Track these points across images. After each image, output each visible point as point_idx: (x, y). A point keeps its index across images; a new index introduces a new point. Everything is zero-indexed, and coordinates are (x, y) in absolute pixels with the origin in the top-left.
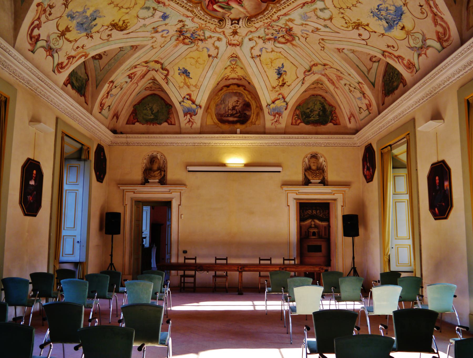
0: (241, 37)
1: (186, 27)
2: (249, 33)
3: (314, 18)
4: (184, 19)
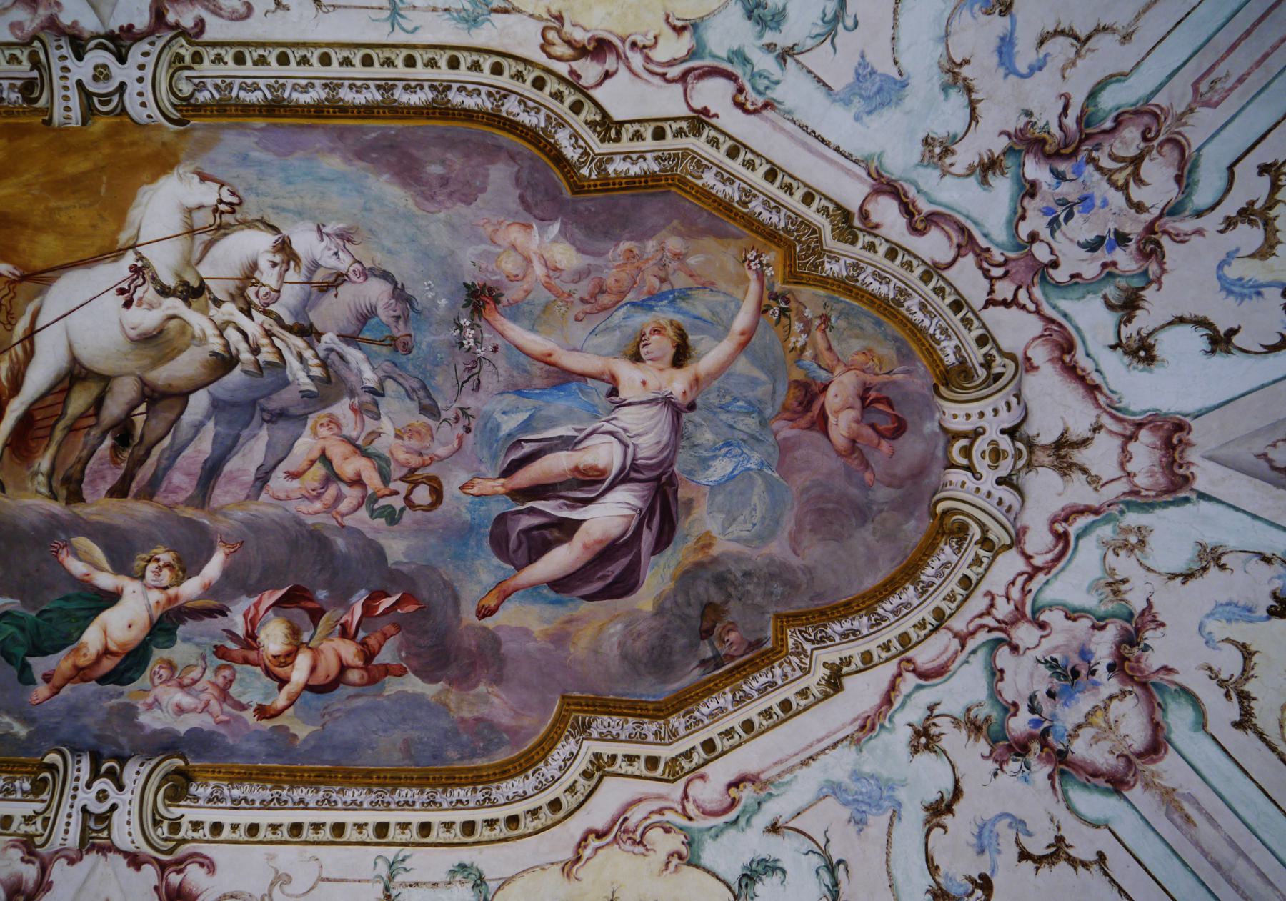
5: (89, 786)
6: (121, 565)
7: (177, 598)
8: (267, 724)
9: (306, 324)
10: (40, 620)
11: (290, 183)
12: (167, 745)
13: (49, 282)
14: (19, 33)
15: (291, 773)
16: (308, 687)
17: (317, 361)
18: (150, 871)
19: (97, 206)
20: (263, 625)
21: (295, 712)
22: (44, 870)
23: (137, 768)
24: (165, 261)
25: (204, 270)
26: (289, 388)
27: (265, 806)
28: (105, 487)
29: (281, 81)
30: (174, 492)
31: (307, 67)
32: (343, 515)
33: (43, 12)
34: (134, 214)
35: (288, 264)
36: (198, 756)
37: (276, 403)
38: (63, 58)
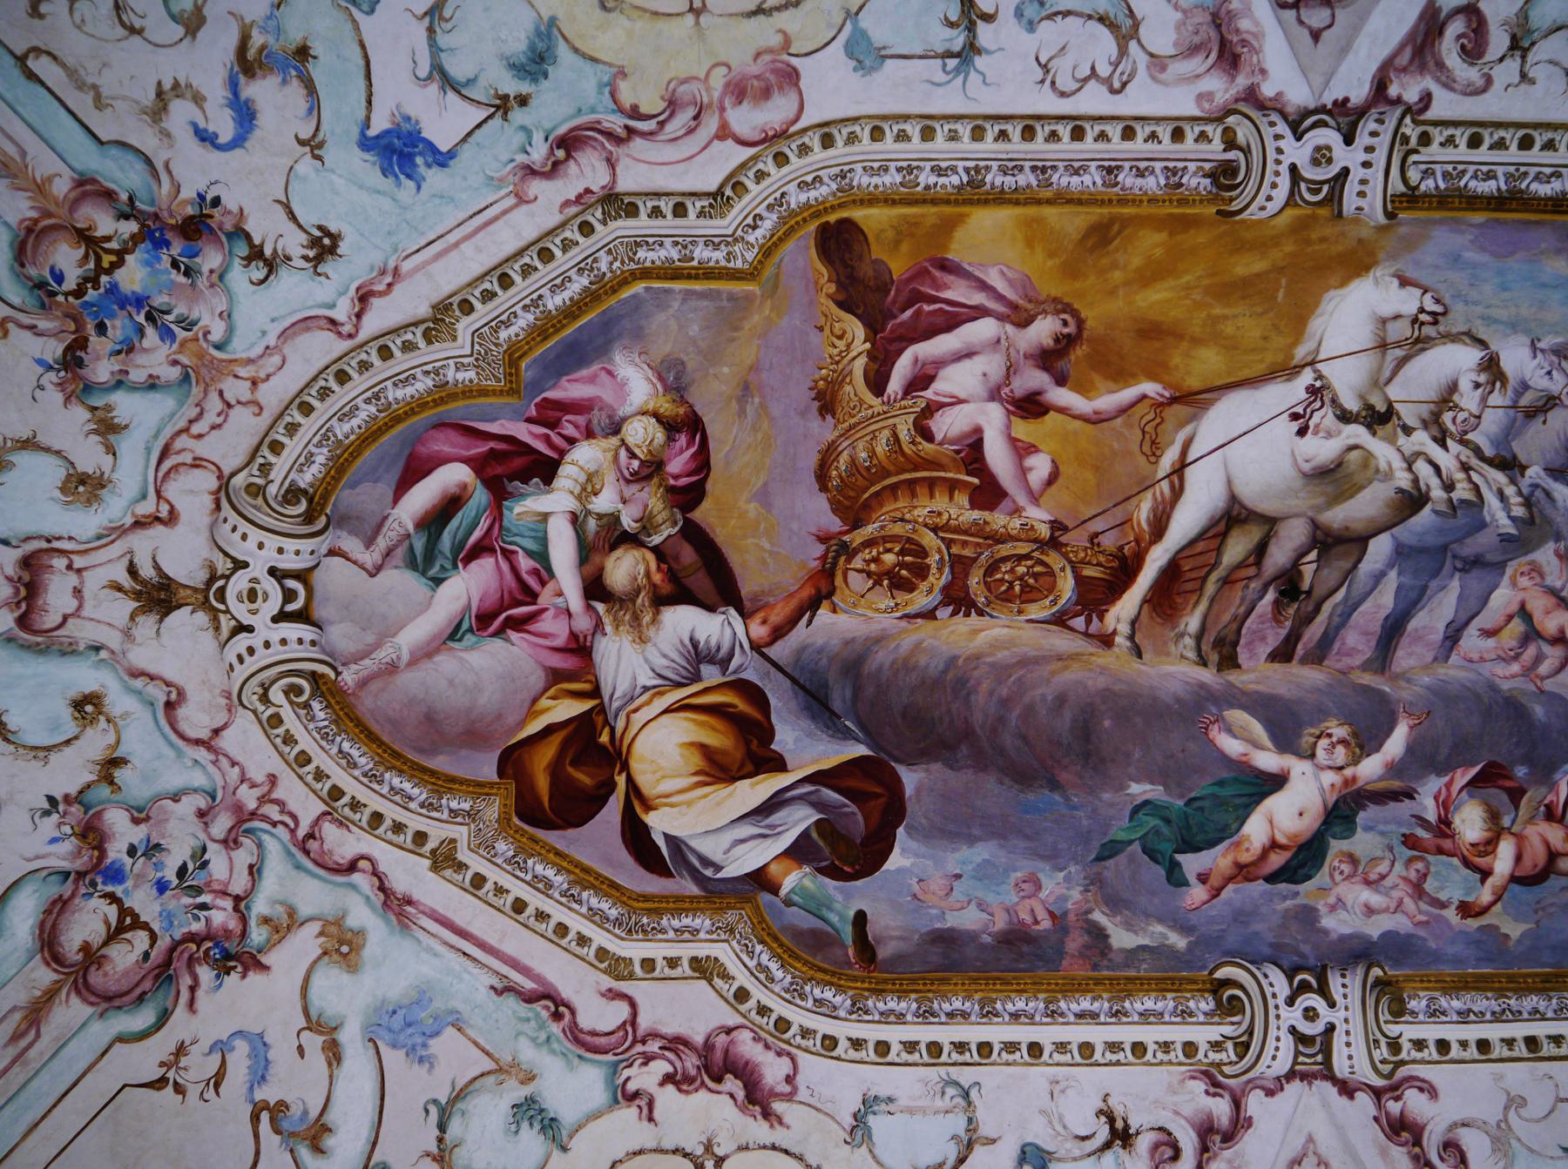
0: (113, 639)
1: (239, 277)
2: (159, 694)
3: (414, 1087)
4: (347, 272)
5: (1291, 1002)
6: (1285, 741)
7: (1354, 779)
8: (1473, 924)
9: (1508, 456)
10: (1189, 810)
11: (1505, 289)
12: (1358, 953)
13: (1205, 406)
14: (1207, 106)
15: (1511, 978)
16: (1514, 879)
17: (1519, 499)
18: (1363, 1098)
19: (1271, 314)
20: (1457, 808)
21: (1504, 908)
22: (1237, 1104)
23: (1340, 980)
24: (1347, 380)
25: (1393, 392)
26: (1486, 530)
27: (1497, 1018)
28: (1264, 650)
29: (1523, 169)
30: (1348, 655)
31: (1551, 153)
32: (1543, 679)
33: (1242, 81)
34: (1316, 325)
35: (1494, 384)
36: (1397, 963)
37: (1470, 548)
38: (1277, 137)
